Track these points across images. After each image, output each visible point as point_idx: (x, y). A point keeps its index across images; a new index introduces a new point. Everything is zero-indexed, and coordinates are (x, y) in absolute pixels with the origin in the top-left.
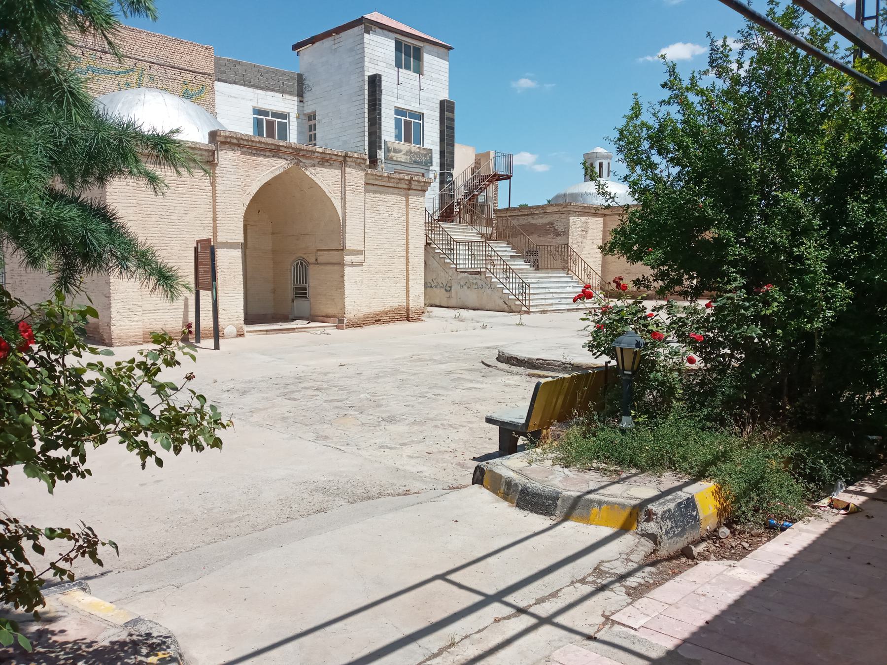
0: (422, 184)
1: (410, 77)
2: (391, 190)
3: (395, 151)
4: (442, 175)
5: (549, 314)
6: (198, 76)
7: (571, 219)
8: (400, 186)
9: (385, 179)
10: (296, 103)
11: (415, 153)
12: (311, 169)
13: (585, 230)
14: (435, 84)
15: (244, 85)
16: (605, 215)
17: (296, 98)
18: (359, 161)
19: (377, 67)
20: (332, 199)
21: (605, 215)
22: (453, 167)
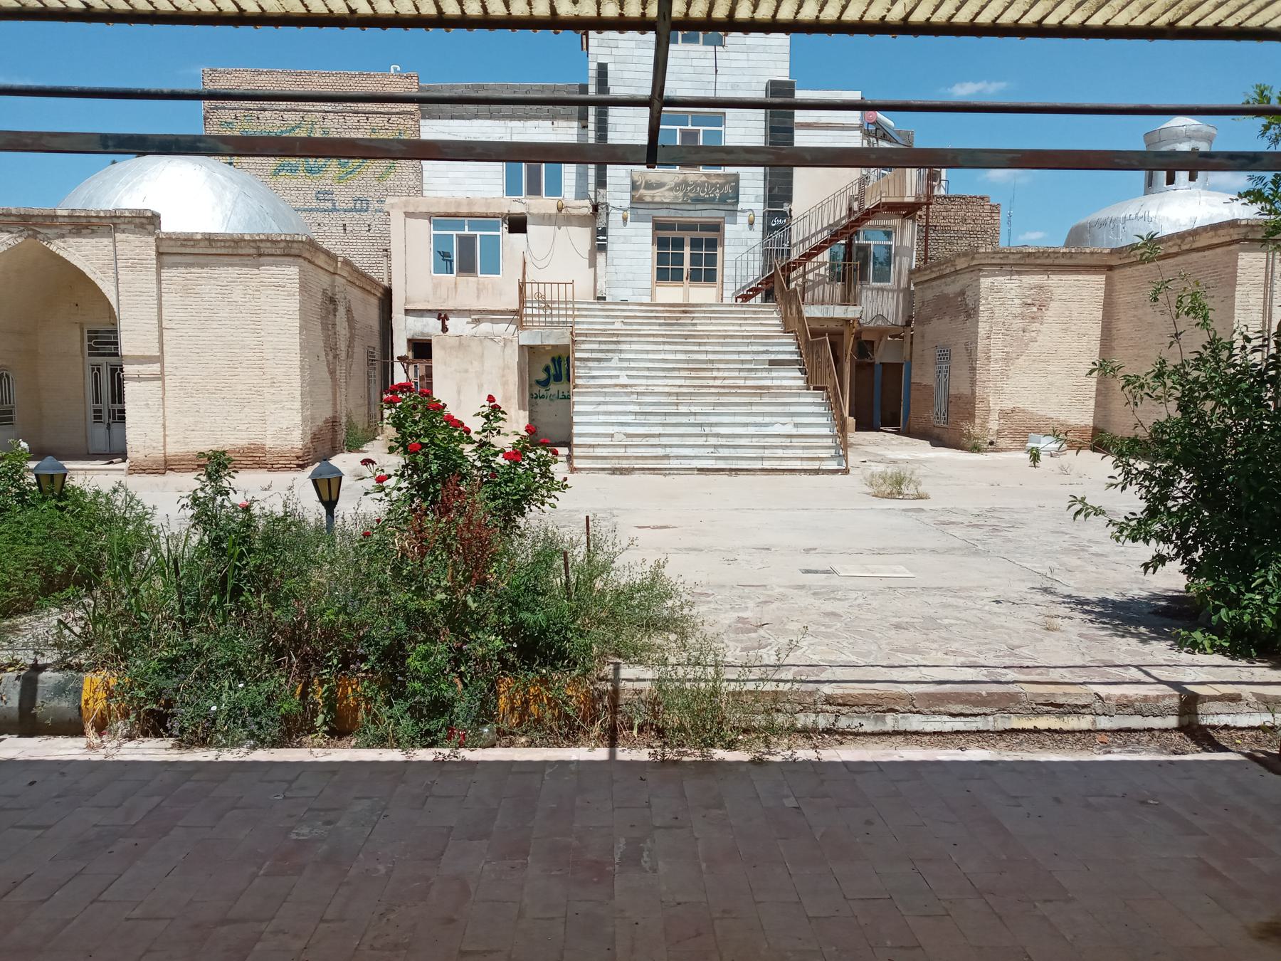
0: (282, 245)
1: (692, 55)
2: (226, 259)
3: (649, 186)
4: (768, 216)
5: (636, 477)
6: (394, 118)
7: (985, 282)
8: (240, 251)
9: (202, 244)
10: (575, 131)
11: (696, 184)
12: (59, 242)
13: (1037, 305)
14: (752, 56)
15: (490, 118)
16: (1111, 268)
17: (575, 124)
18: (137, 220)
19: (615, 51)
20: (99, 283)
21: (1111, 268)
22: (789, 200)
